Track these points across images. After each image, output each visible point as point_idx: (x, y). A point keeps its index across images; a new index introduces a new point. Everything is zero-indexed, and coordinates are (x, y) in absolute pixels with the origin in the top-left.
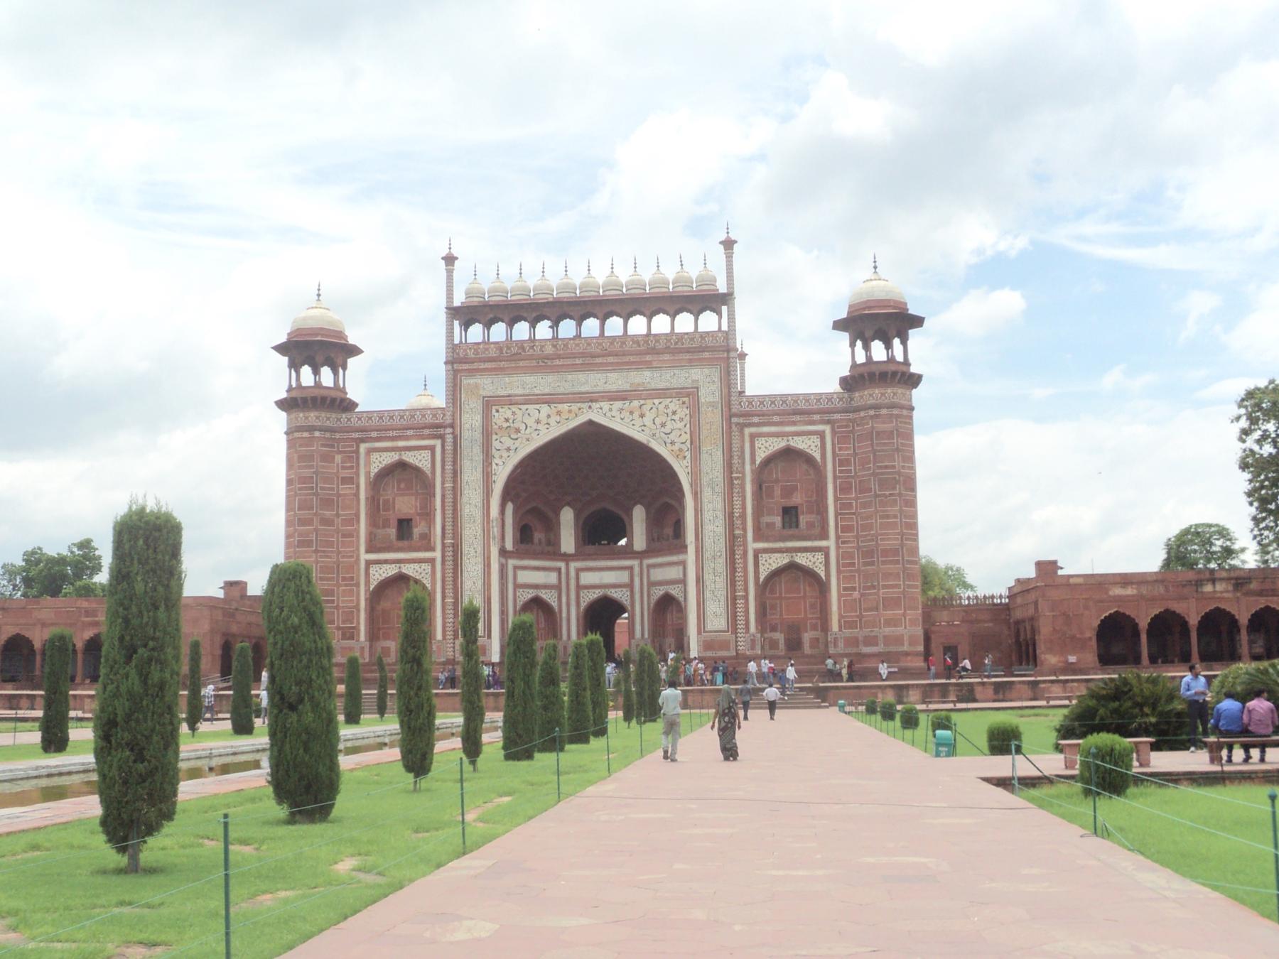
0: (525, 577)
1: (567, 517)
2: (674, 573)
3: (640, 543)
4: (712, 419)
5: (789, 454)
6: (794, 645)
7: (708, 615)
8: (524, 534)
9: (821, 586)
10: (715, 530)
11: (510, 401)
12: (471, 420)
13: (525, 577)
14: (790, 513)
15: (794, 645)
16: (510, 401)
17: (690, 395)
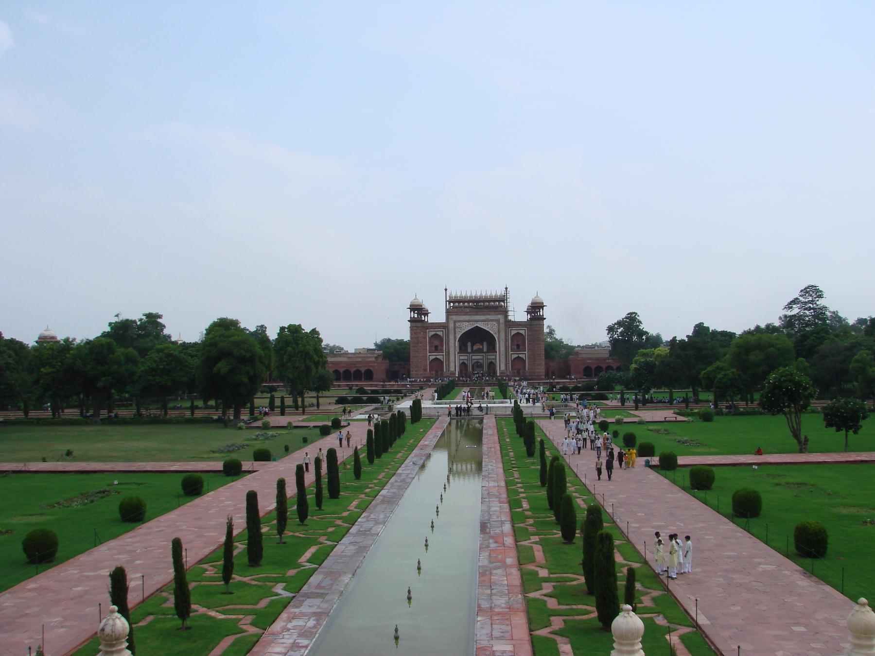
0: (462, 358)
1: (469, 344)
2: (493, 357)
3: (485, 350)
4: (502, 326)
5: (518, 333)
6: (519, 373)
7: (501, 367)
8: (460, 349)
9: (525, 361)
10: (503, 349)
11: (460, 321)
12: (451, 325)
13: (462, 358)
14: (518, 346)
15: (519, 373)
16: (460, 321)
17: (498, 321)
